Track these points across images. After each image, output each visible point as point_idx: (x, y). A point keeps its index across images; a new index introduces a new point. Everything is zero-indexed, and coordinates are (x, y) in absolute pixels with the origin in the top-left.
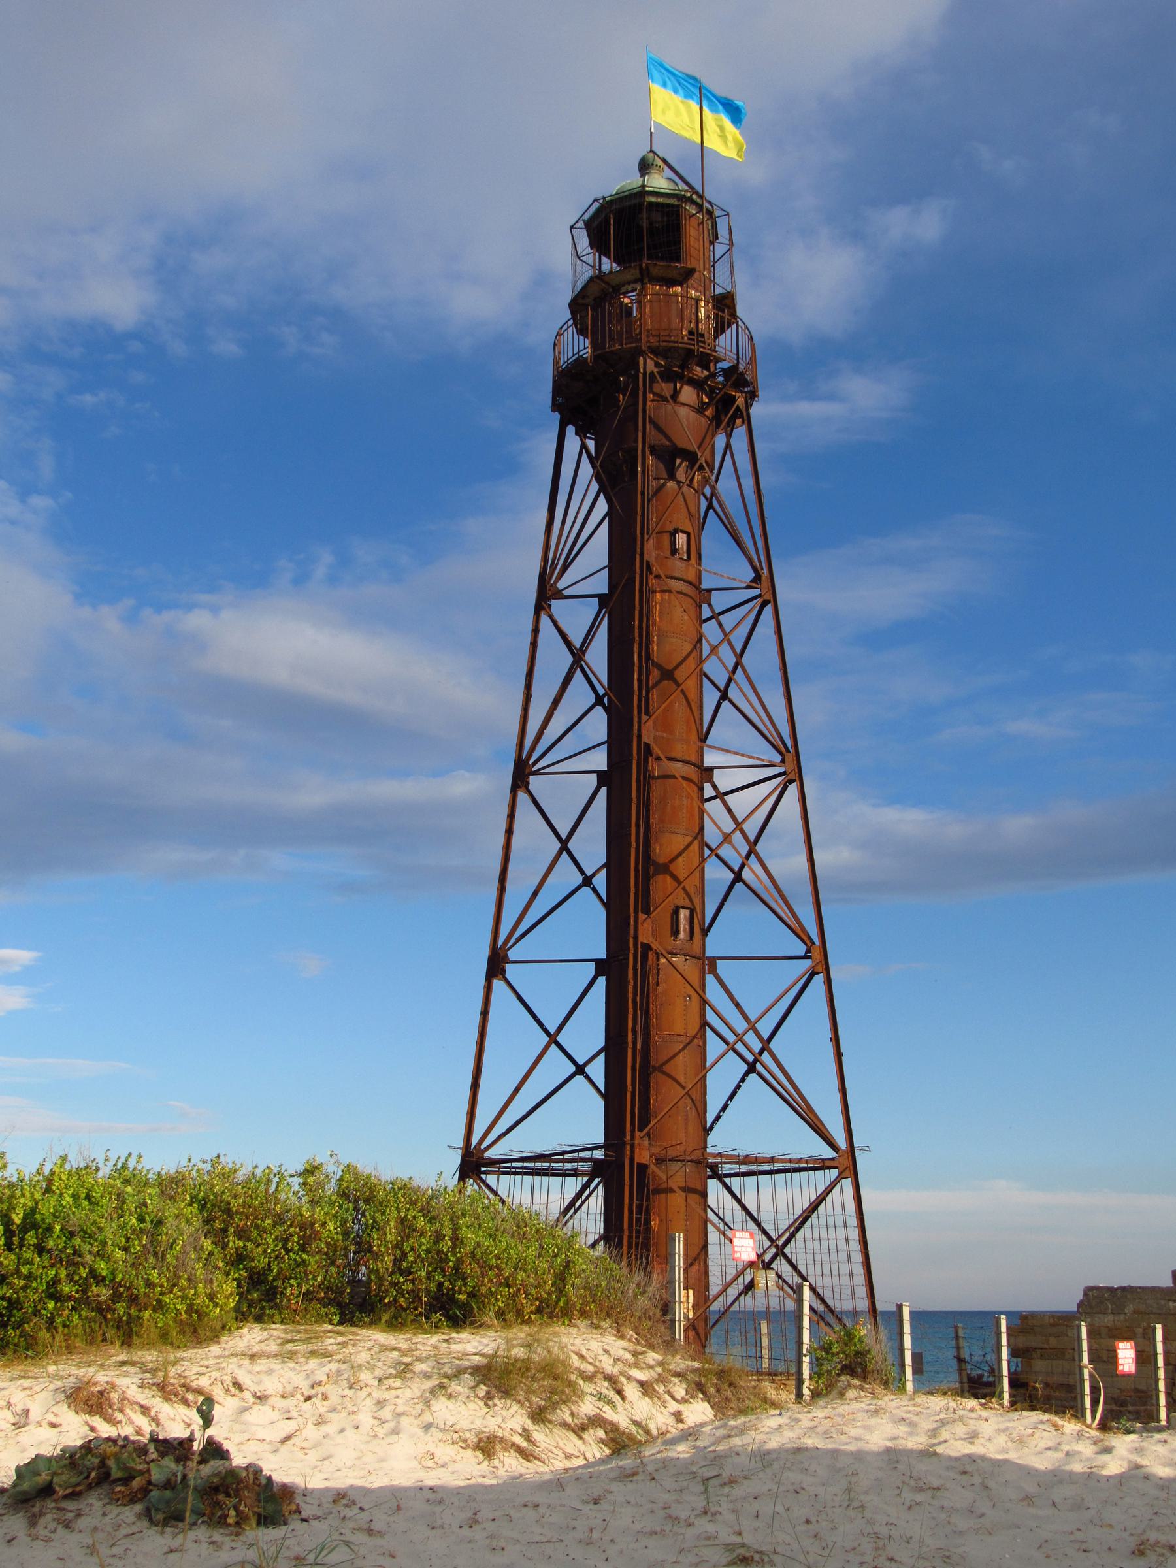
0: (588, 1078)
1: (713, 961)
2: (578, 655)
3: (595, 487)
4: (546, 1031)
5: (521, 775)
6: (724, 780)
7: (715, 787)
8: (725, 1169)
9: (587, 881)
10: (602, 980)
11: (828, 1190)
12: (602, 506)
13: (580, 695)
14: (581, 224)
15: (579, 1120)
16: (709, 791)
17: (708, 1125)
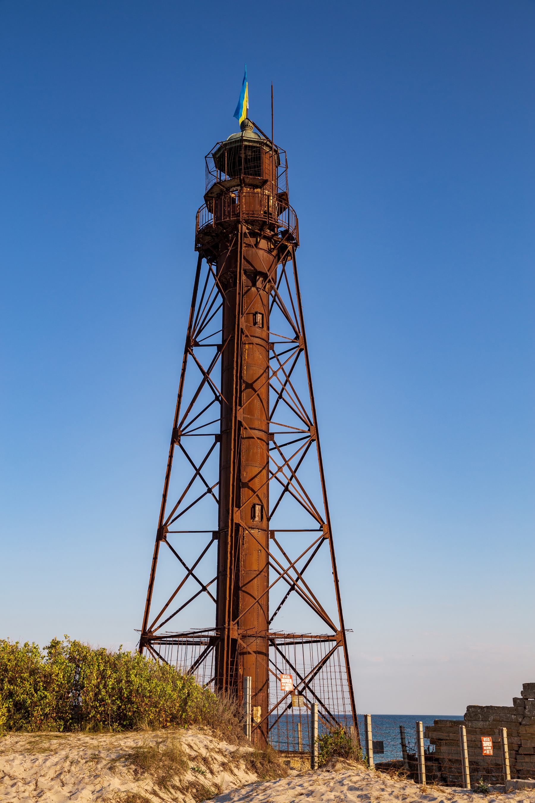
0: (208, 592)
1: (273, 532)
2: (206, 375)
3: (216, 290)
4: (187, 568)
5: (176, 436)
6: (279, 439)
7: (275, 443)
8: (278, 641)
9: (210, 491)
10: (216, 542)
11: (331, 653)
13: (207, 395)
14: (211, 155)
15: (203, 615)
16: (272, 445)
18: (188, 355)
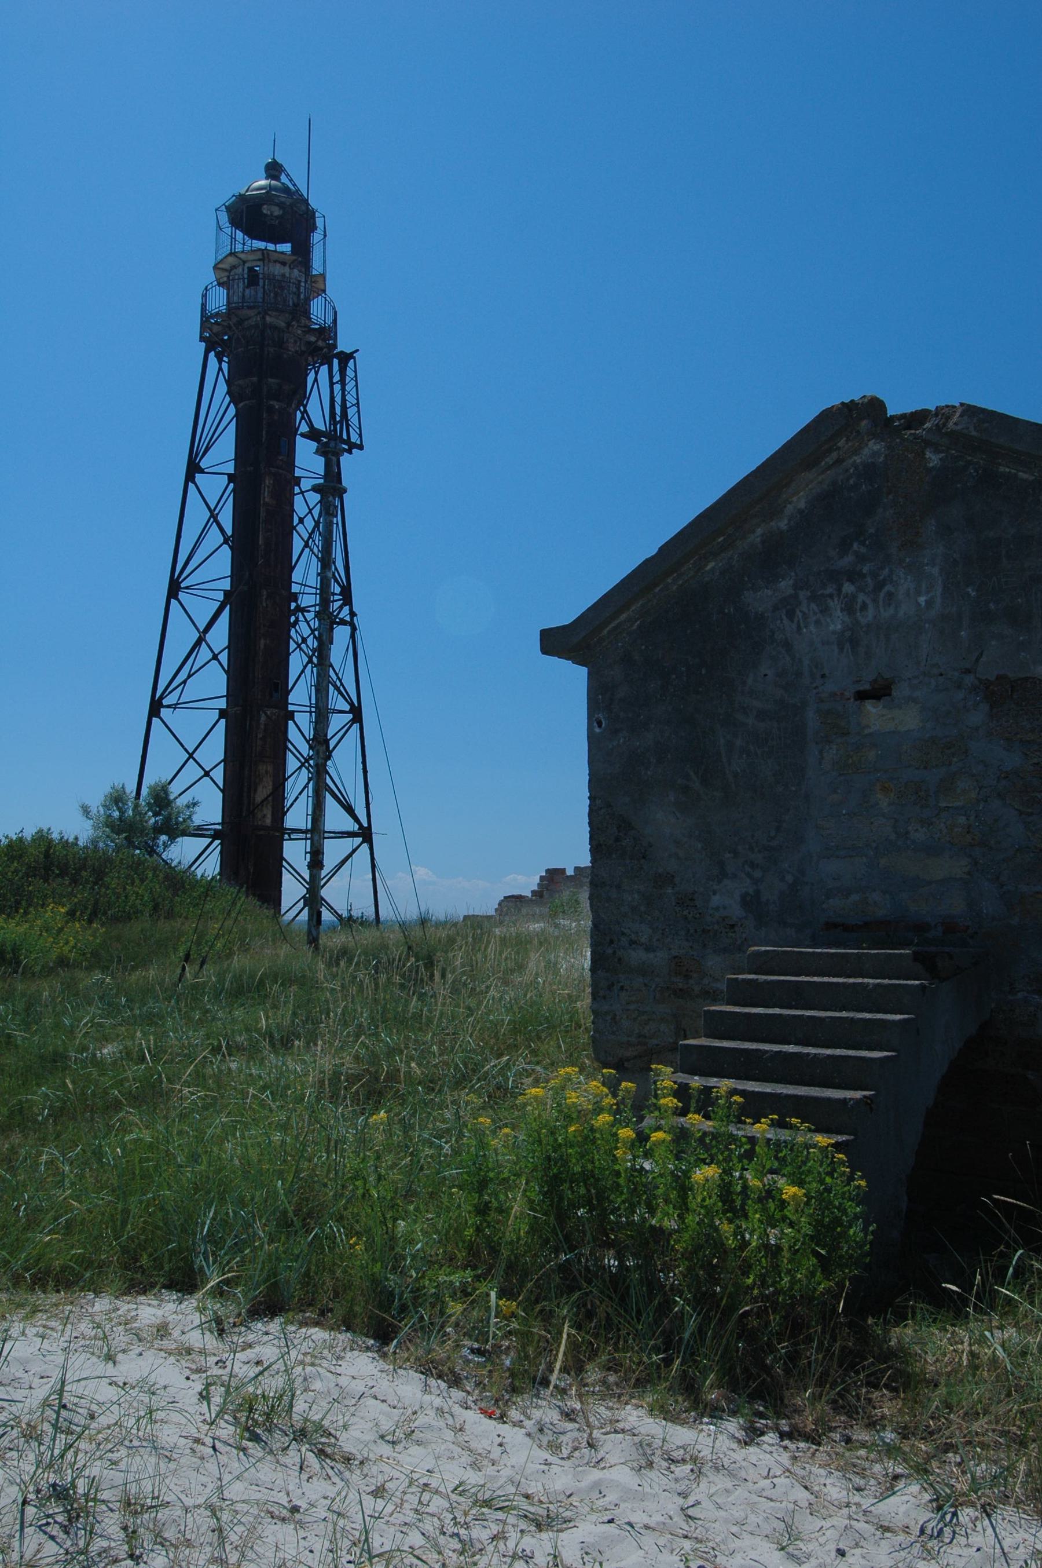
0: (212, 779)
2: (214, 516)
3: (228, 399)
5: (174, 589)
9: (215, 657)
10: (223, 721)
13: (214, 537)
14: (223, 208)
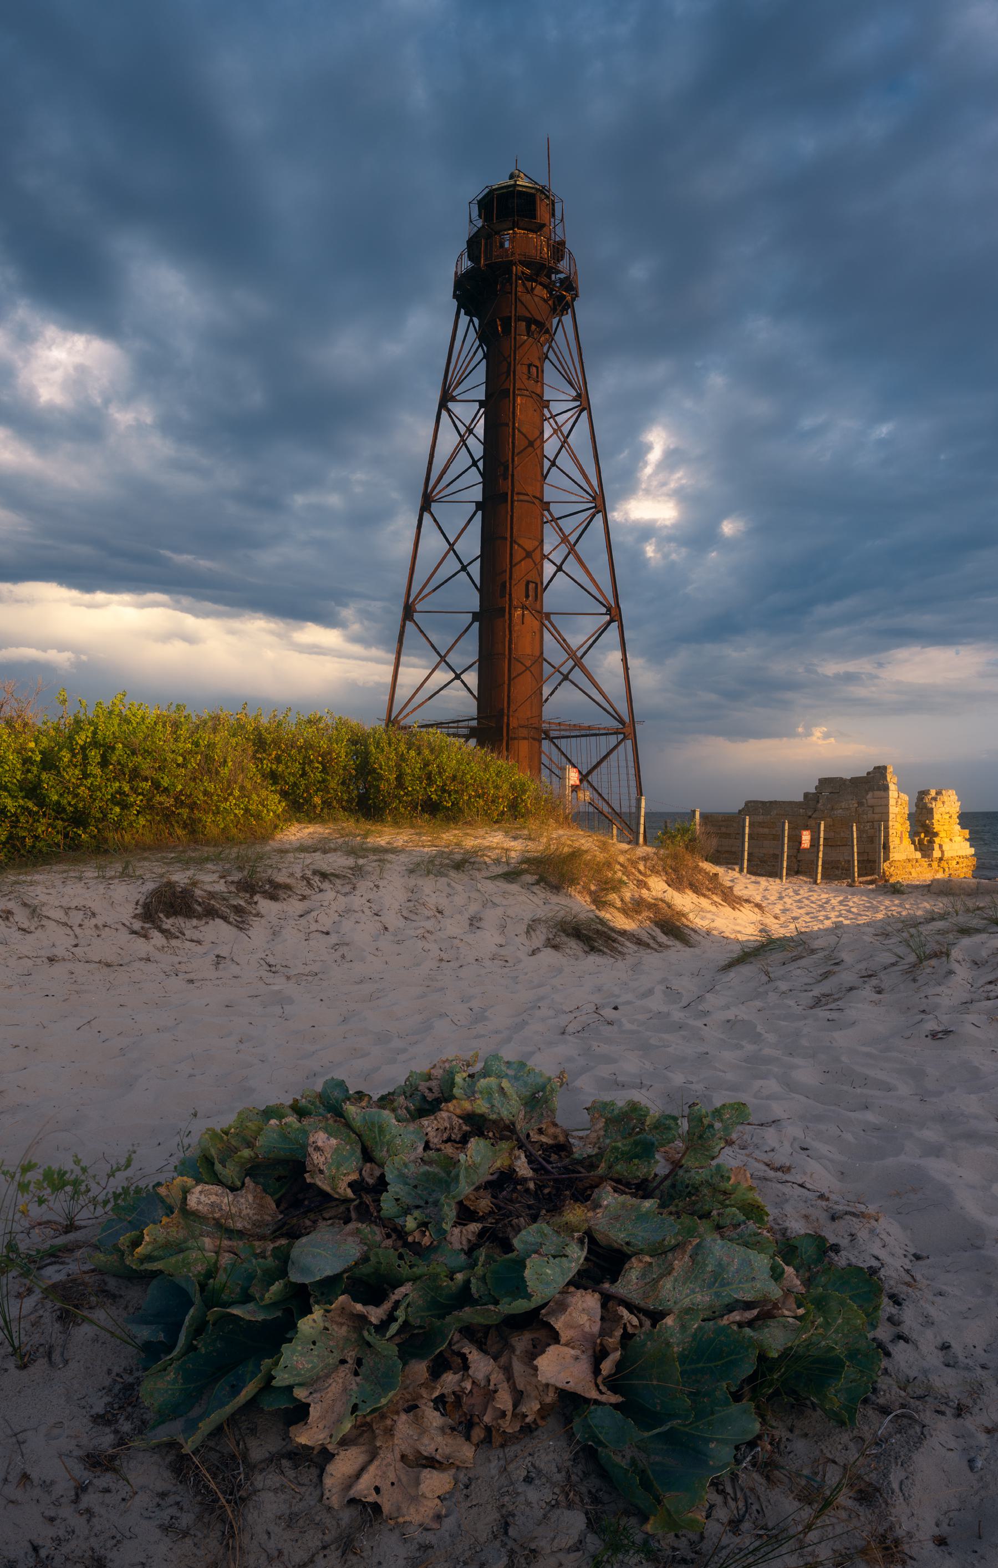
1: (548, 615)
3: (477, 343)
4: (438, 653)
5: (427, 503)
6: (557, 510)
7: (551, 514)
10: (476, 624)
11: (619, 744)
12: (480, 354)
14: (475, 202)
17: (544, 698)
18: (444, 413)
